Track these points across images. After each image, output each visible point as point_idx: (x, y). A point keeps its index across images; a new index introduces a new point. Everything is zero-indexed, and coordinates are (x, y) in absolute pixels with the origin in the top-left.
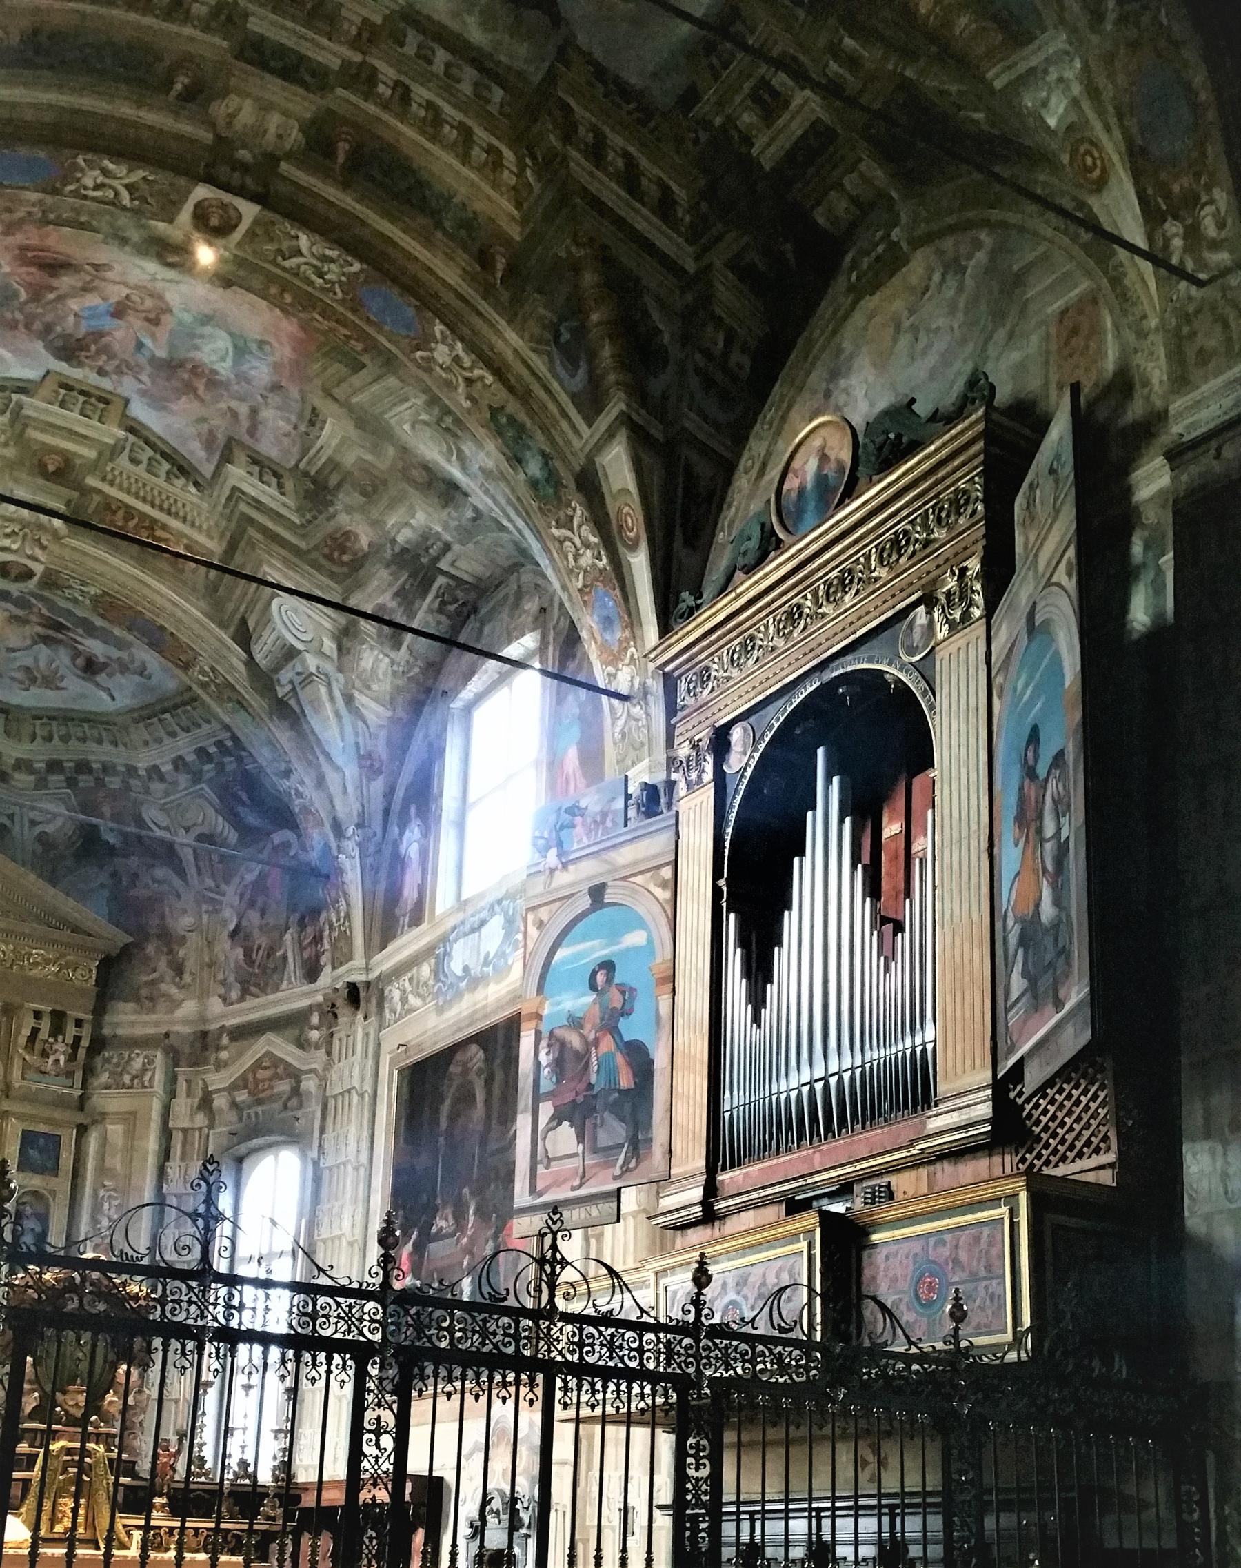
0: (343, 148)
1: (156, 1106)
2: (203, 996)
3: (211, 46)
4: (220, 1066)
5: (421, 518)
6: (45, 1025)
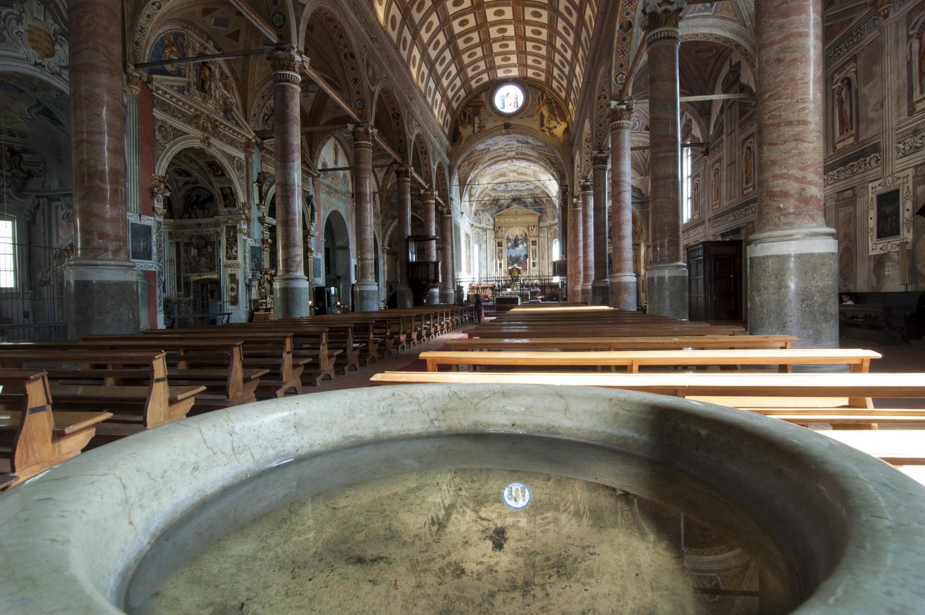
3: (504, 153)
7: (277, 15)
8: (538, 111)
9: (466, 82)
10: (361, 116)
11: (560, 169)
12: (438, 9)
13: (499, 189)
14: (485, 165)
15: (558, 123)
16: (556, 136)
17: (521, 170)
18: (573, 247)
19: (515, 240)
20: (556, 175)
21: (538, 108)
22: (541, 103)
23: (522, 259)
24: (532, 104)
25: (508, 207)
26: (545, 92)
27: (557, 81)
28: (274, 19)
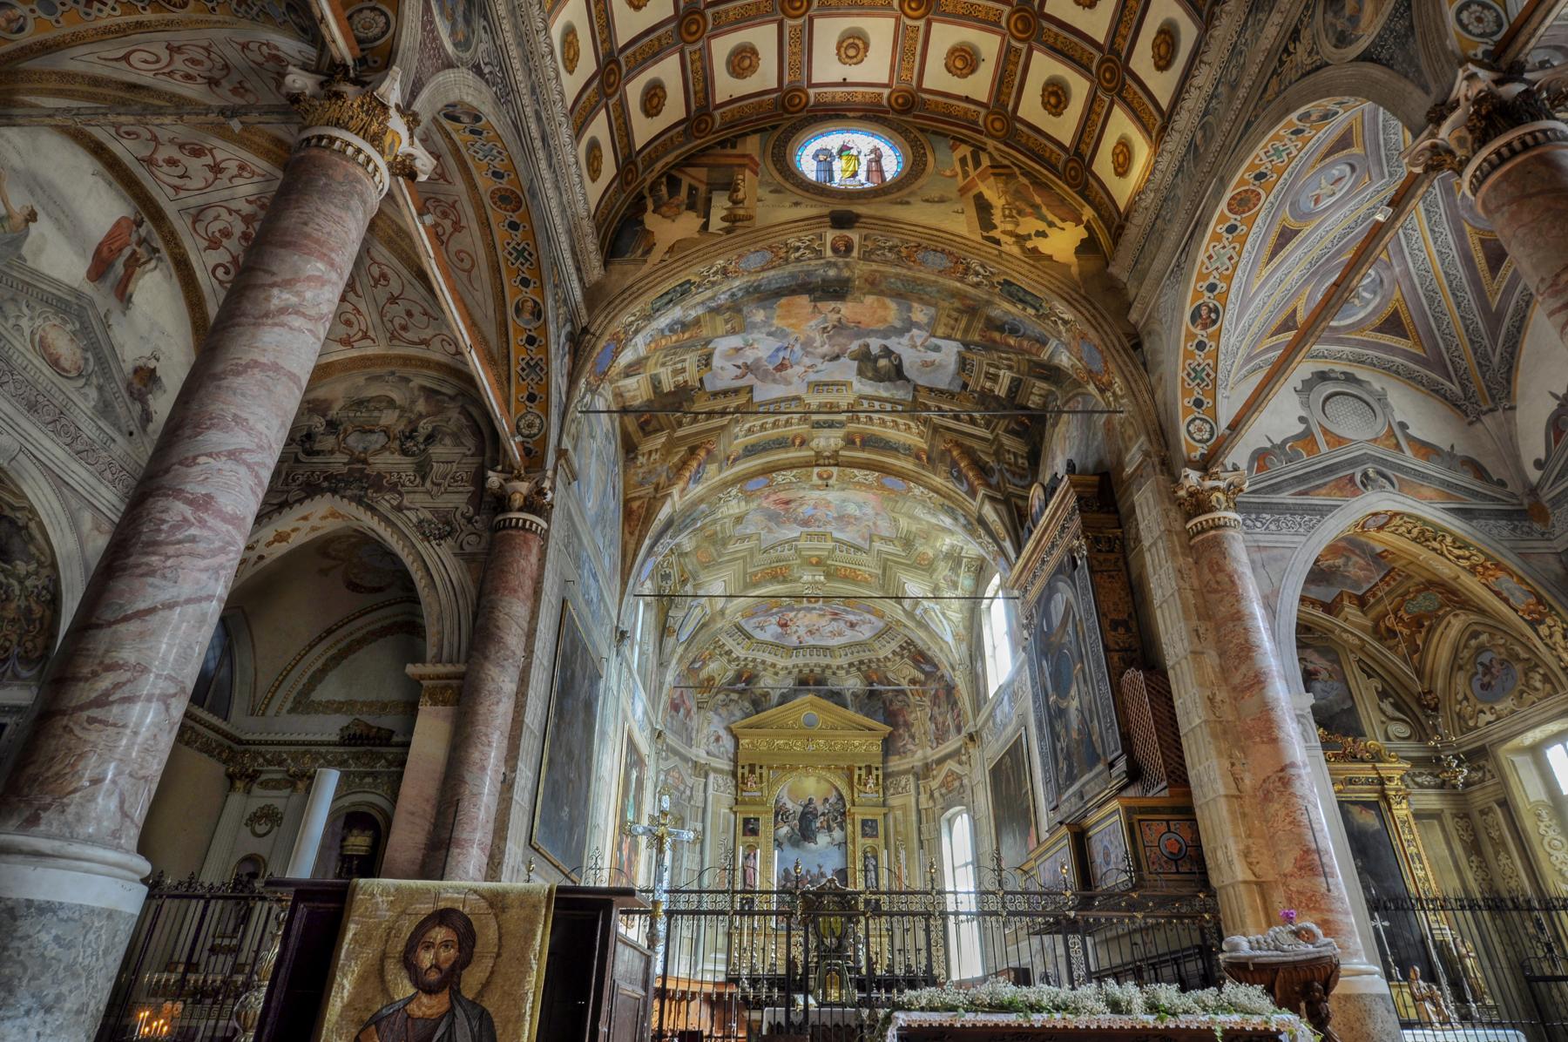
0: (858, 441)
1: (913, 800)
2: (923, 748)
4: (934, 778)
5: (948, 541)
6: (863, 772)
11: (1011, 489)
13: (758, 634)
14: (729, 473)
18: (1228, 714)
19: (804, 814)
21: (960, 181)
22: (972, 173)
25: (784, 699)
26: (984, 150)
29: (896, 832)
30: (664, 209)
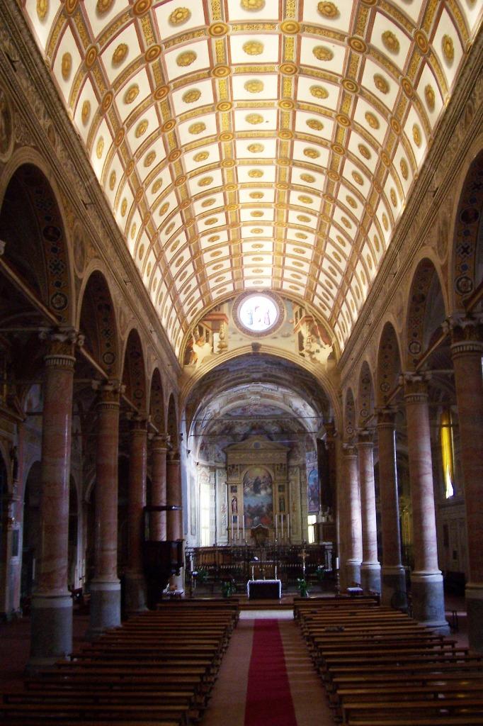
3: (248, 374)
6: (279, 467)
7: (58, 296)
8: (295, 330)
9: (205, 293)
10: (109, 372)
12: (188, 229)
15: (322, 346)
16: (319, 362)
17: (266, 392)
20: (315, 404)
21: (295, 326)
22: (299, 321)
23: (264, 509)
24: (288, 321)
25: (246, 437)
26: (304, 308)
27: (320, 298)
28: (54, 301)
29: (292, 490)
30: (199, 342)
